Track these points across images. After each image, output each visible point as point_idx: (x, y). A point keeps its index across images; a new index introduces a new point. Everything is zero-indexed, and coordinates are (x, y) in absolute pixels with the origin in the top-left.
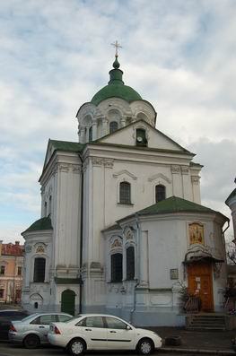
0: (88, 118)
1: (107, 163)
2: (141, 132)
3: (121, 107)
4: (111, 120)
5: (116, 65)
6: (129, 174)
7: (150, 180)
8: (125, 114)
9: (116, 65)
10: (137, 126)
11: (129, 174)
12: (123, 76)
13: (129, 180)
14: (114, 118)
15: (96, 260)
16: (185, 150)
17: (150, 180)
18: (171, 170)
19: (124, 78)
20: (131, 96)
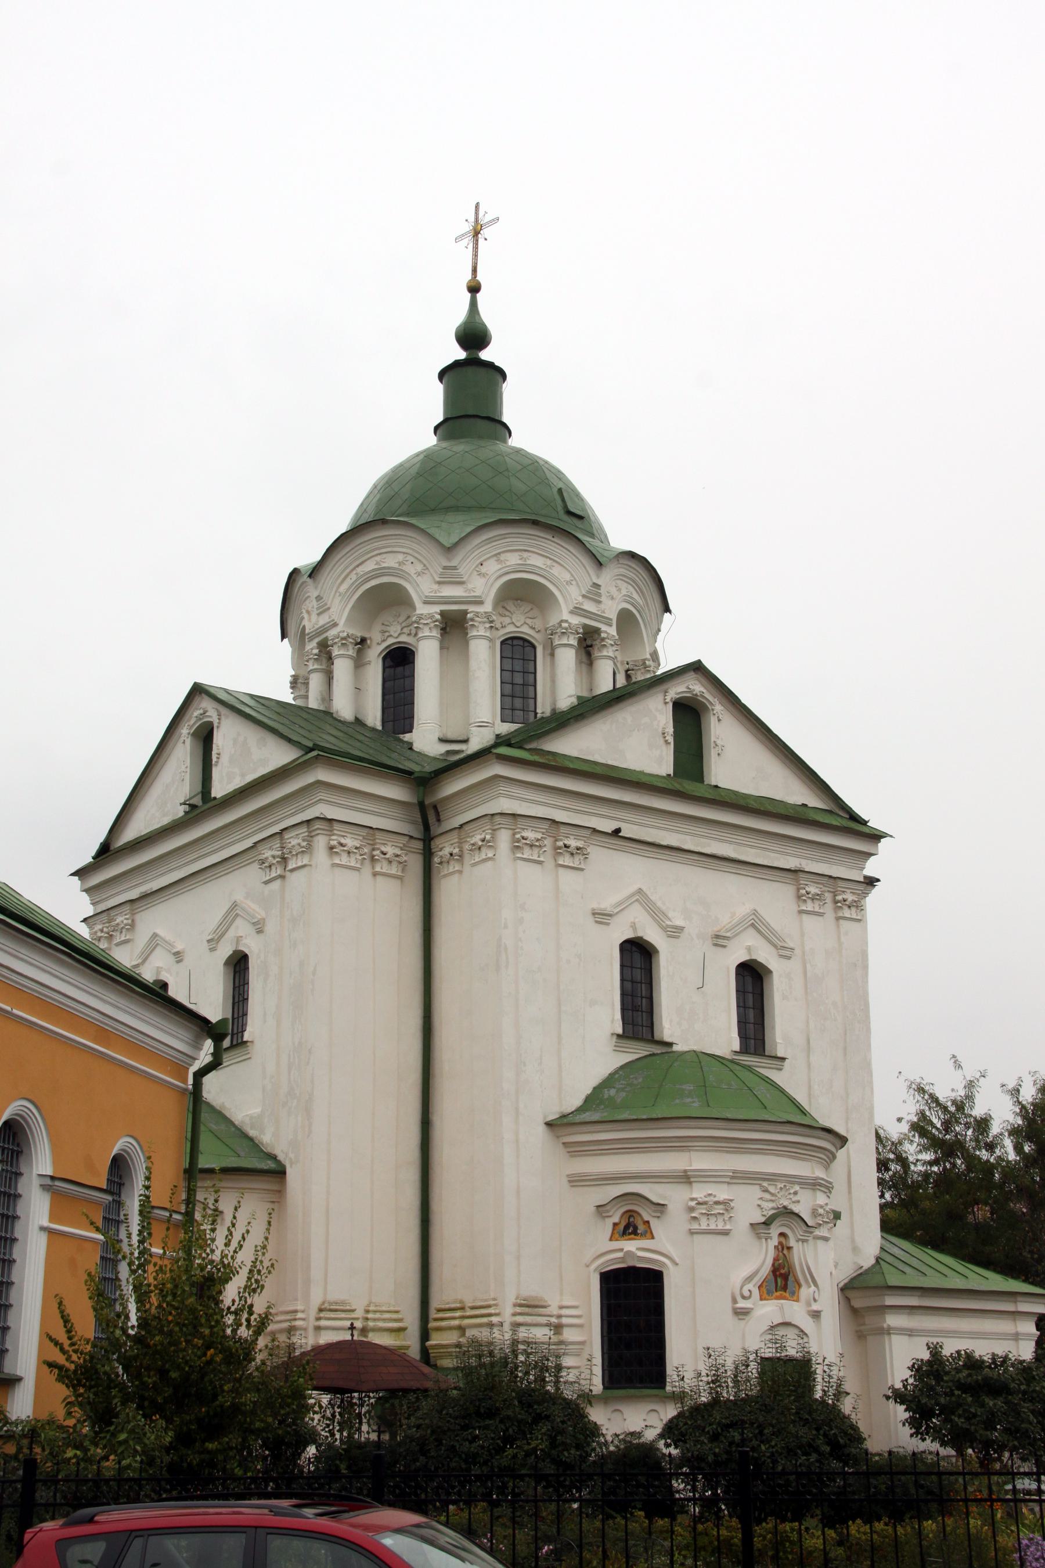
0: (385, 599)
1: (563, 844)
2: (689, 716)
3: (556, 571)
4: (510, 630)
5: (473, 336)
6: (657, 914)
7: (719, 940)
8: (577, 611)
9: (473, 336)
10: (677, 690)
11: (657, 914)
12: (510, 392)
13: (653, 935)
14: (520, 623)
15: (531, 1289)
16: (854, 817)
17: (719, 940)
18: (799, 897)
19: (515, 406)
20: (556, 514)
